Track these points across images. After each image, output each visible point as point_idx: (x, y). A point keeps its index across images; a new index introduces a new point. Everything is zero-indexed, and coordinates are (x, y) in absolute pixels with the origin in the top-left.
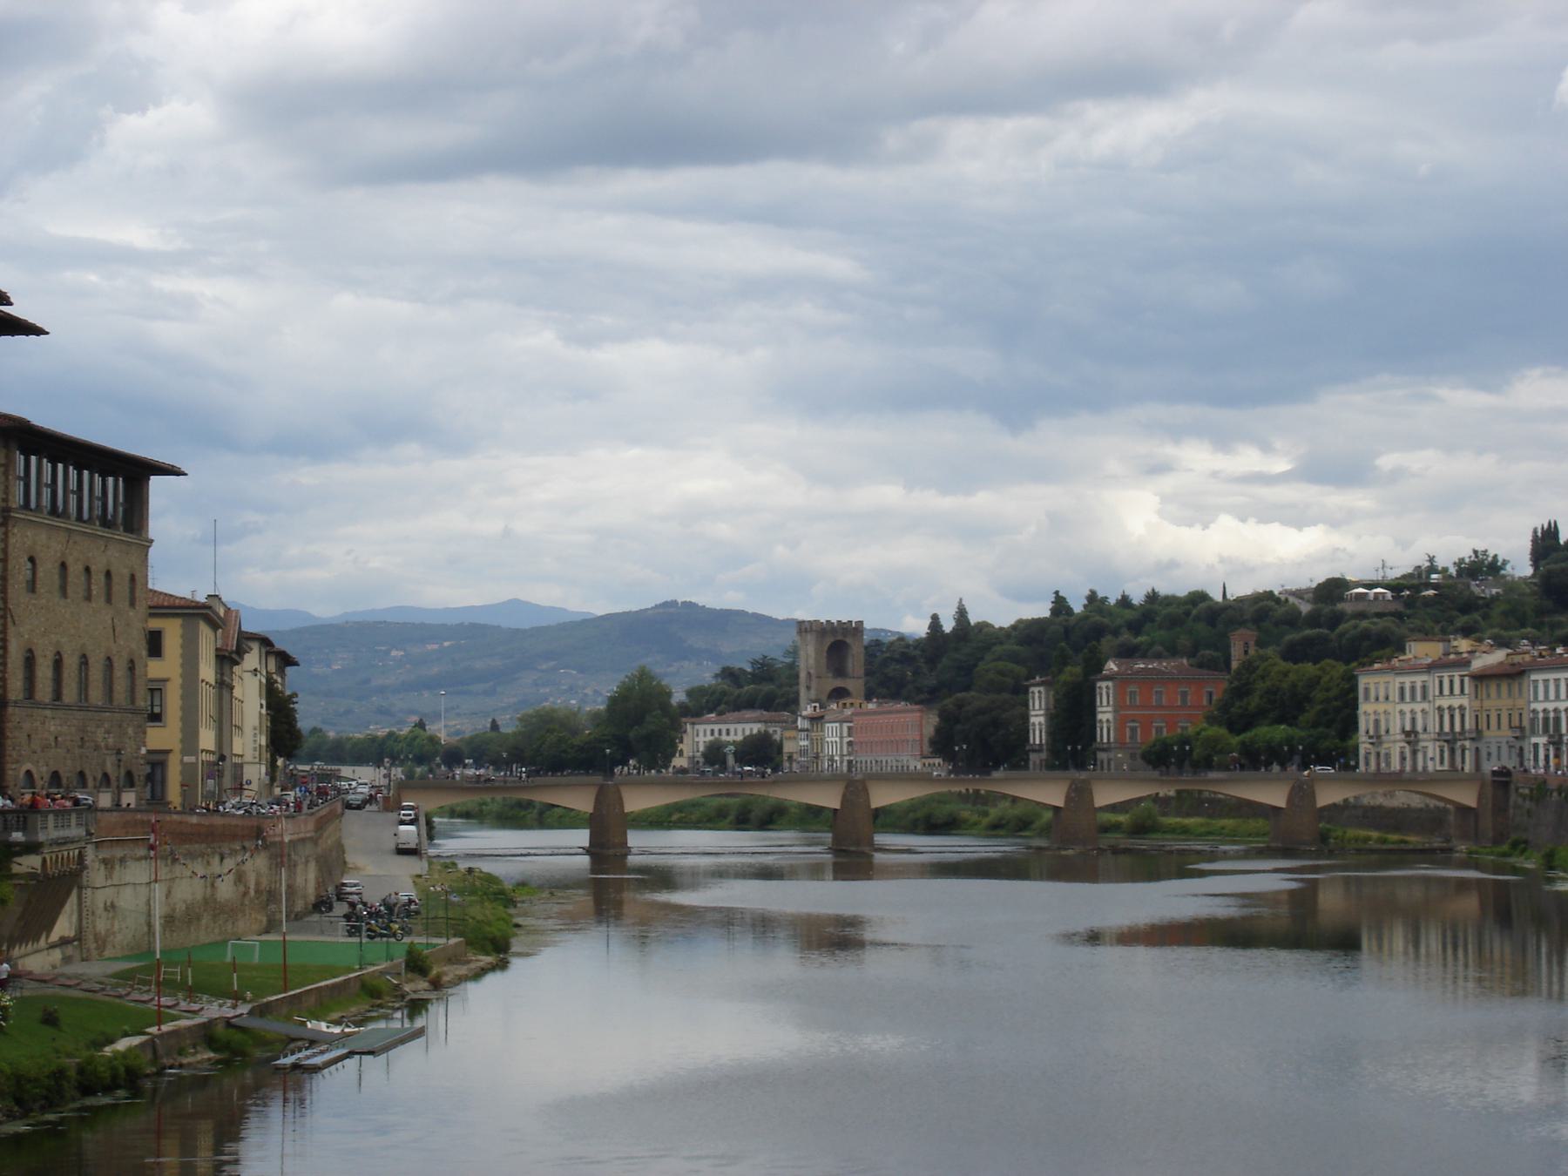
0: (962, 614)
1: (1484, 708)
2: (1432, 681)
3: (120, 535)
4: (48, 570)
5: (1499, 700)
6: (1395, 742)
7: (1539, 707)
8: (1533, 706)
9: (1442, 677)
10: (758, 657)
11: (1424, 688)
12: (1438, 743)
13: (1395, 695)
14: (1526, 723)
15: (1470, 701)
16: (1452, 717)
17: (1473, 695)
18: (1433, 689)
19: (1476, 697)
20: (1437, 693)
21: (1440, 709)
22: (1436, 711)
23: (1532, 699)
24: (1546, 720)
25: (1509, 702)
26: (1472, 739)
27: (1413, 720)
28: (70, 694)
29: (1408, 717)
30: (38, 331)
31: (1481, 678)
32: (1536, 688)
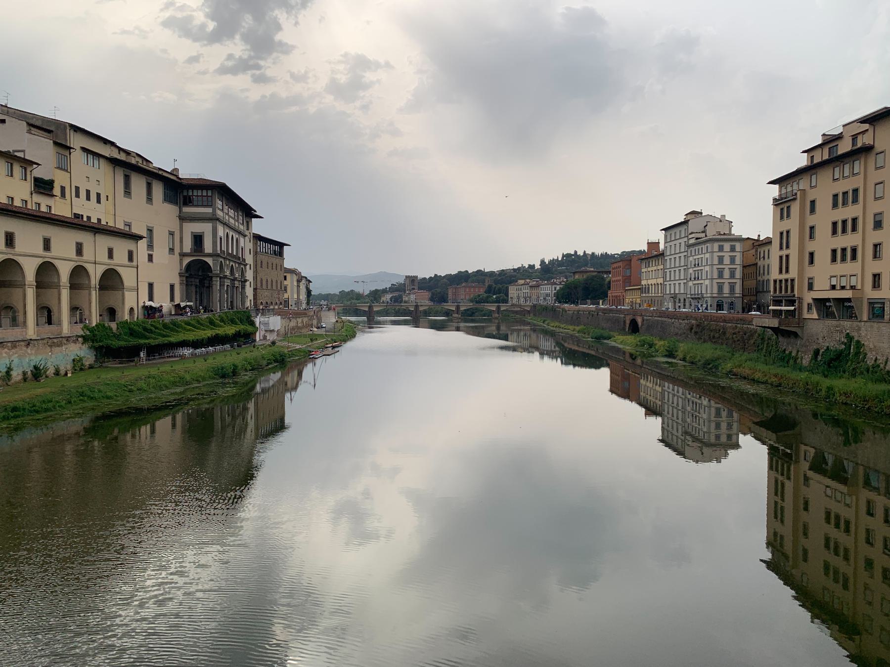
3: (278, 257)
4: (265, 264)
5: (535, 291)
7: (542, 292)
13: (515, 290)
28: (269, 287)
30: (262, 218)
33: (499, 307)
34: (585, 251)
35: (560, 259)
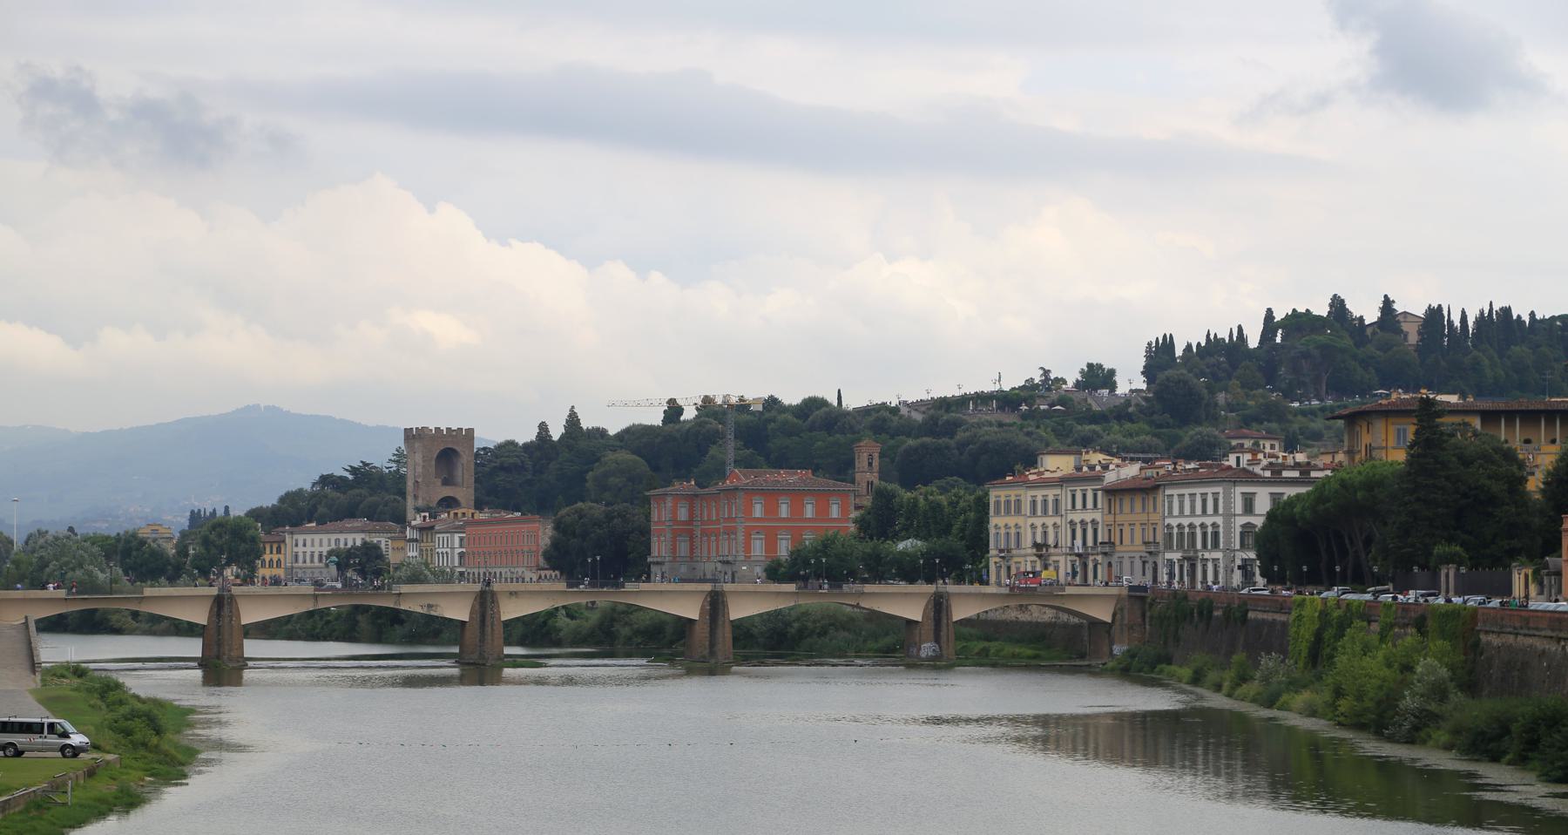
0: (573, 421)
1: (1117, 523)
2: (1065, 495)
5: (1132, 514)
6: (1025, 556)
7: (1174, 522)
8: (1167, 521)
9: (1076, 490)
10: (357, 464)
11: (1056, 501)
12: (1069, 558)
13: (1026, 508)
14: (1159, 538)
15: (1102, 517)
16: (1084, 531)
17: (1106, 511)
18: (1066, 503)
19: (1110, 512)
20: (1069, 507)
21: (1072, 523)
22: (1068, 525)
24: (1181, 534)
25: (1144, 518)
26: (1105, 554)
27: (1045, 533)
29: (1039, 530)
31: (1113, 492)
32: (1171, 504)
33: (939, 606)
34: (1387, 304)
35: (1253, 342)
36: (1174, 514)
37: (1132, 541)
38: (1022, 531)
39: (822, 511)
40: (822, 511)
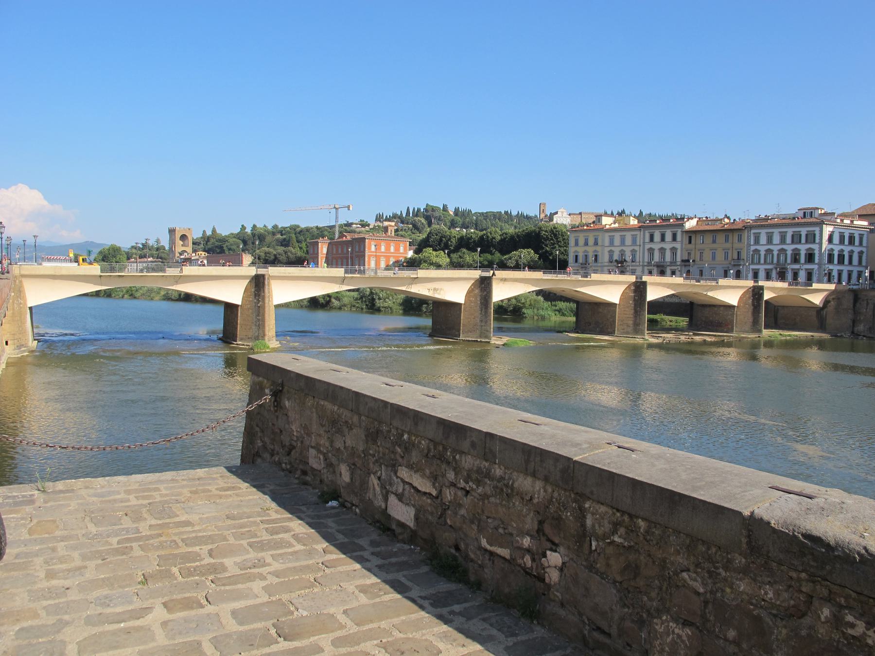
0: (214, 230)
12: (646, 268)
15: (682, 246)
17: (686, 240)
19: (690, 242)
20: (647, 239)
23: (752, 243)
36: (761, 243)
37: (714, 258)
38: (599, 254)
39: (397, 249)
40: (397, 249)
